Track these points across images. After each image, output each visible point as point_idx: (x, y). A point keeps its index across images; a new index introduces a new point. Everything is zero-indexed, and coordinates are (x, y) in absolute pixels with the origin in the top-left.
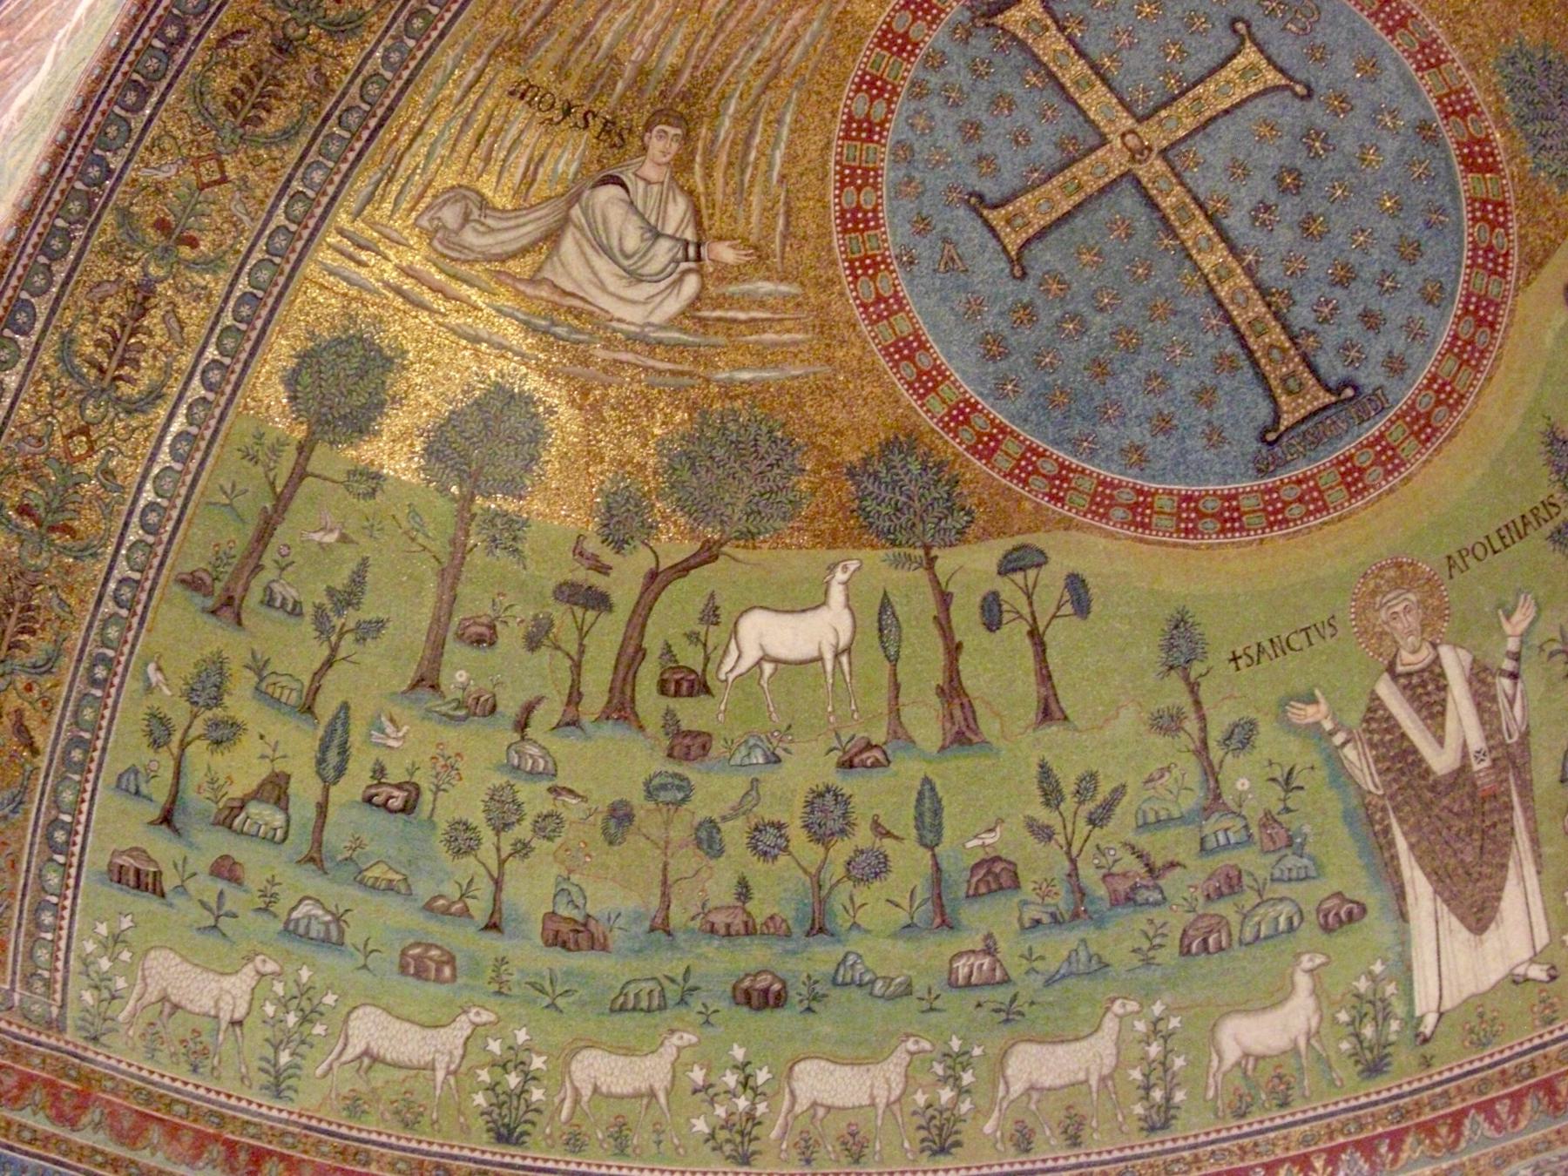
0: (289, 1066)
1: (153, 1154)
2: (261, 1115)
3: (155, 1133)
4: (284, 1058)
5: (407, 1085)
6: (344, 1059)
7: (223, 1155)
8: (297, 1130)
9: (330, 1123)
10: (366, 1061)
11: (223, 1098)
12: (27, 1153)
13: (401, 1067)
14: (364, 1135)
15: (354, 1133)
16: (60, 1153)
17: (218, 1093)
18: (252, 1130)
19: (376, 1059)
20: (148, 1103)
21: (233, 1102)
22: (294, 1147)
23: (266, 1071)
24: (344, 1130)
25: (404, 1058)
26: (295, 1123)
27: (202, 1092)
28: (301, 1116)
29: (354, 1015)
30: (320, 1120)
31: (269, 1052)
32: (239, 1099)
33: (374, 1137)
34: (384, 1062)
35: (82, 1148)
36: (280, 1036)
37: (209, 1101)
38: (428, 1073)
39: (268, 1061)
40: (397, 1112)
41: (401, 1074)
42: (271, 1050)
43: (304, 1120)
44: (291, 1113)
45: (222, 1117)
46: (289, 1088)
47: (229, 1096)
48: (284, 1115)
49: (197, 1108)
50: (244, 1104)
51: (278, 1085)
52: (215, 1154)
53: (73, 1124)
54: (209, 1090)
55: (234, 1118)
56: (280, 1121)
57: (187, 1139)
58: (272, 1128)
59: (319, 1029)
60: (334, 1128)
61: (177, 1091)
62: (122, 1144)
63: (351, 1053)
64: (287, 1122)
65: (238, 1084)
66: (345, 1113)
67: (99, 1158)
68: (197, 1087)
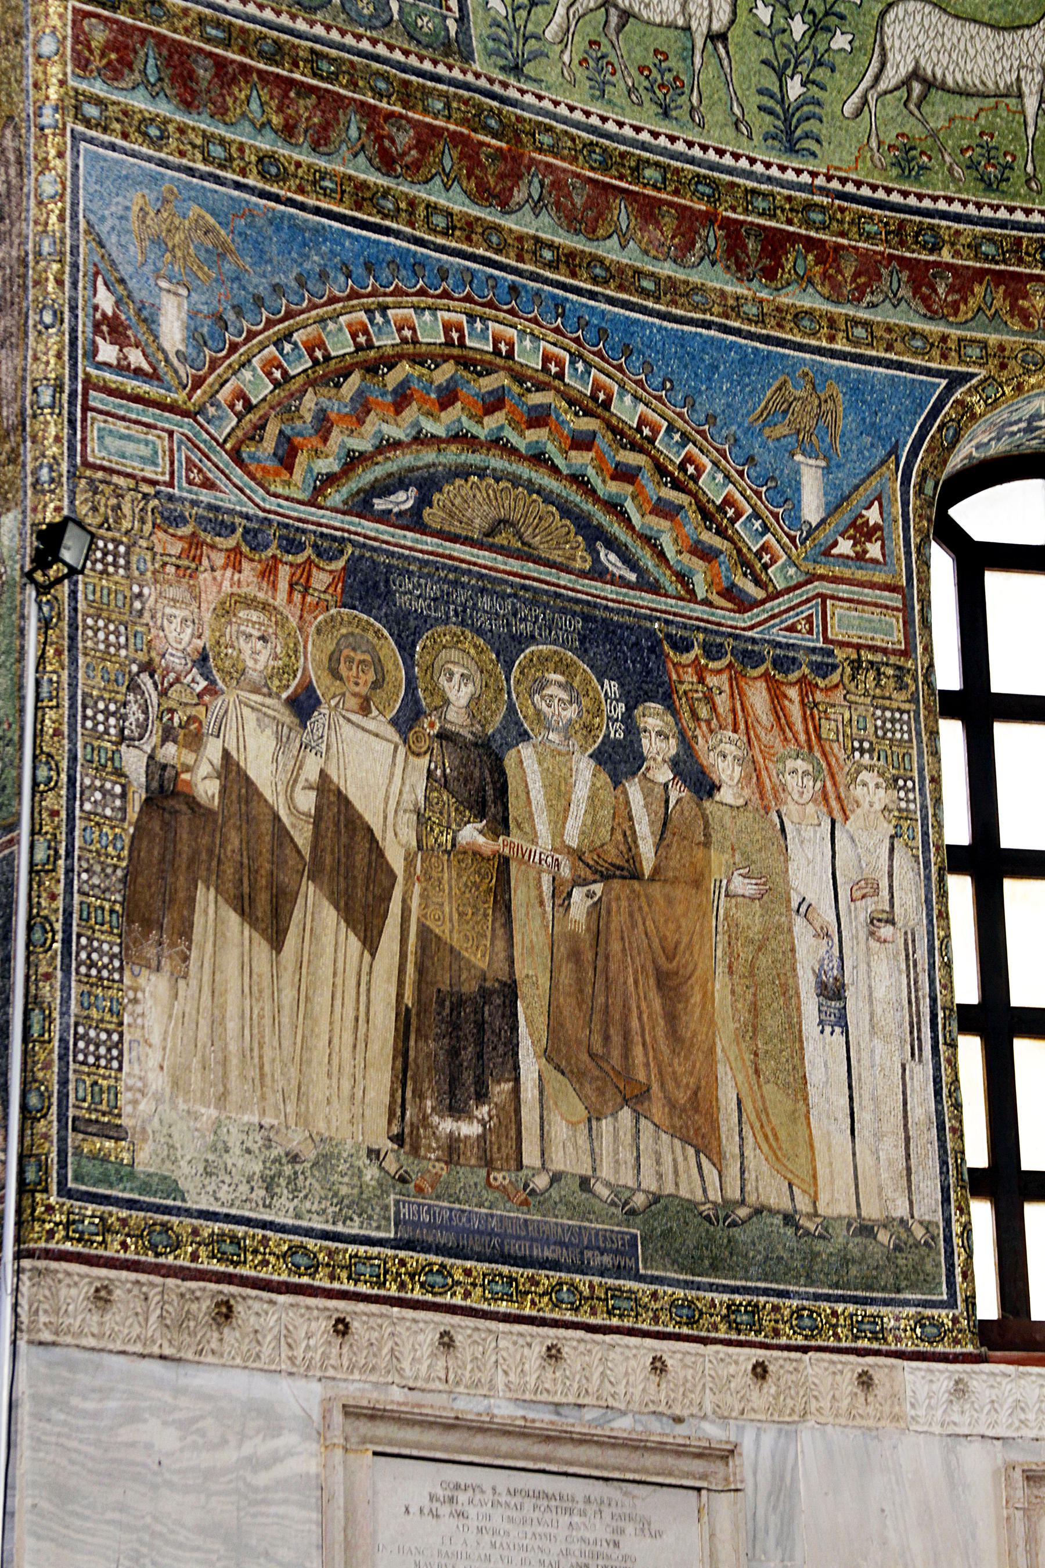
0: (804, 101)
1: (623, 247)
2: (770, 180)
3: (622, 215)
4: (795, 89)
5: (982, 121)
6: (882, 86)
7: (723, 242)
8: (826, 201)
9: (874, 188)
10: (917, 87)
11: (712, 155)
12: (443, 249)
13: (969, 95)
14: (927, 203)
15: (912, 201)
16: (489, 248)
17: (704, 148)
18: (761, 204)
19: (930, 84)
20: (604, 167)
21: (728, 160)
22: (824, 227)
23: (771, 112)
24: (895, 198)
25: (973, 81)
26: (824, 191)
27: (680, 146)
28: (829, 178)
29: (890, 16)
30: (858, 184)
31: (771, 82)
32: (736, 157)
33: (942, 205)
34: (943, 87)
35: (520, 239)
36: (784, 54)
37: (692, 161)
38: (1012, 102)
39: (772, 96)
40: (972, 165)
41: (971, 106)
42: (774, 78)
43: (835, 185)
44: (814, 175)
45: (714, 184)
46: (807, 136)
47: (721, 153)
48: (805, 178)
49: (677, 171)
50: (744, 163)
51: (790, 133)
52: (712, 242)
53: (504, 204)
54: (690, 144)
55: (733, 185)
56: (801, 187)
57: (669, 223)
58: (789, 199)
59: (840, 42)
60: (880, 194)
61: (644, 146)
62: (577, 232)
63: (892, 77)
64: (810, 189)
65: (730, 132)
66: (894, 172)
67: (548, 255)
68: (673, 139)
